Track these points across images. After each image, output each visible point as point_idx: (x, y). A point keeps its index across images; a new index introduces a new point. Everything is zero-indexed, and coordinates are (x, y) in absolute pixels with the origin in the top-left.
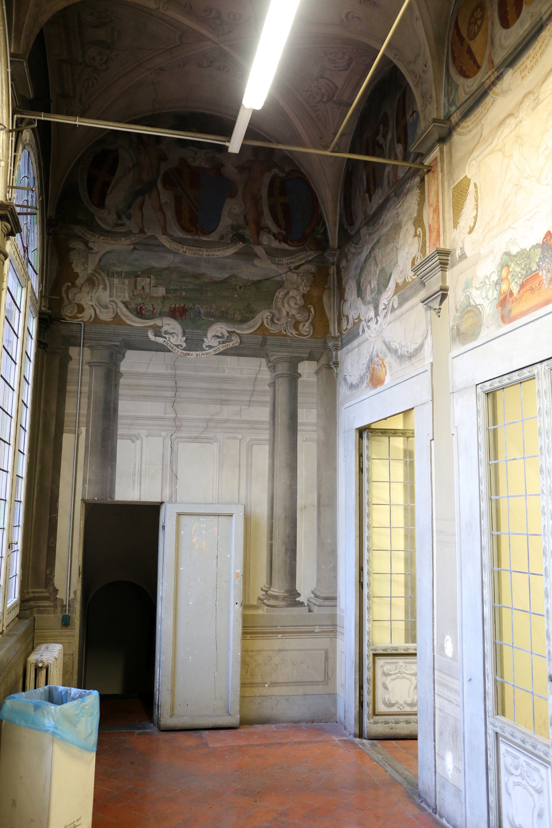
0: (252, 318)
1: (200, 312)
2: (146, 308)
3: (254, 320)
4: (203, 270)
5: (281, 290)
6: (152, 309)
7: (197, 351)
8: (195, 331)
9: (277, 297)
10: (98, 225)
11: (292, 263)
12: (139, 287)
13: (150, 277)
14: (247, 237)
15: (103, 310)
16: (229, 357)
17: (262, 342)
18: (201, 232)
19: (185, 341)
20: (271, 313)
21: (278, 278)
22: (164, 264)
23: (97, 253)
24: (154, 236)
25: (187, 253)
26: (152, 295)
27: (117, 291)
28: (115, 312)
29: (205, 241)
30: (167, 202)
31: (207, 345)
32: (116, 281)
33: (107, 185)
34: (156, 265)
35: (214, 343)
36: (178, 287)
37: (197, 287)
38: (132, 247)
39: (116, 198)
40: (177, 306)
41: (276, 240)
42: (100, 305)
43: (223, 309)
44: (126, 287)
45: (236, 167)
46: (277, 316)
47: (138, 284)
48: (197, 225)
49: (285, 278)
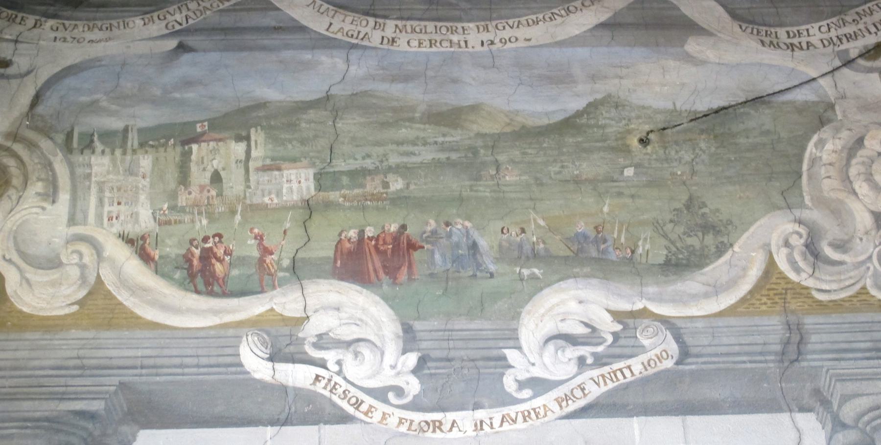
0: (721, 250)
1: (474, 247)
2: (227, 252)
4: (471, 93)
5: (826, 132)
6: (256, 254)
7: (477, 406)
8: (460, 324)
9: (814, 161)
11: (849, 38)
12: (199, 177)
13: (248, 138)
15: (36, 276)
16: (636, 426)
17: (787, 343)
19: (415, 371)
20: (800, 222)
21: (802, 95)
22: (307, 87)
23: (28, 73)
25: (402, 45)
26: (256, 200)
27: (101, 201)
28: (92, 279)
31: (523, 376)
32: (100, 164)
34: (272, 94)
35: (559, 364)
36: (369, 164)
37: (454, 156)
38: (173, 43)
40: (370, 232)
43: (581, 227)
44: (146, 182)
46: (831, 230)
47: (194, 168)
49: (831, 94)
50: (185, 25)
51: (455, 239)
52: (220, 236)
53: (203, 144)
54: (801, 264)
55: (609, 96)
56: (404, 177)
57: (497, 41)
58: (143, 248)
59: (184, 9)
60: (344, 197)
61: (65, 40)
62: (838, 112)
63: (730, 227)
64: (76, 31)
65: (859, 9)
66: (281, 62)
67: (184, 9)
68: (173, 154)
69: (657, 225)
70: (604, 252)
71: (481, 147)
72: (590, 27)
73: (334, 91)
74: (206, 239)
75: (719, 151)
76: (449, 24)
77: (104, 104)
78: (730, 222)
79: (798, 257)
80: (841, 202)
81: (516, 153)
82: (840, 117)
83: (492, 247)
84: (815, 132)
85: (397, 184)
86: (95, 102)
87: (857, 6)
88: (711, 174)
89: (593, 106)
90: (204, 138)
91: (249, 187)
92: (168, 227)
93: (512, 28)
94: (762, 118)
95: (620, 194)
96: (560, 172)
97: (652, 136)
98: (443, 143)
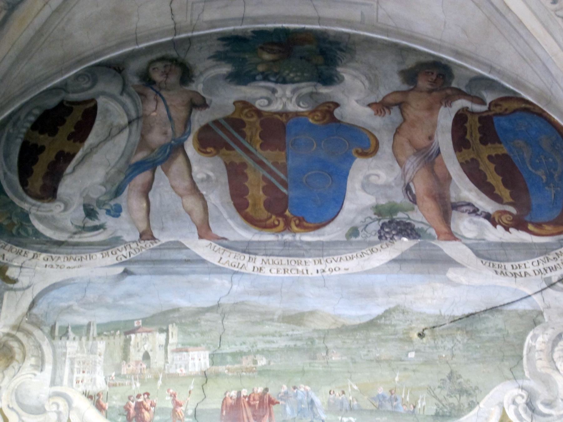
0: (472, 406)
1: (312, 403)
3: (476, 410)
4: (311, 302)
5: (538, 330)
6: (171, 406)
9: (530, 349)
10: (37, 233)
11: (551, 269)
12: (135, 355)
13: (167, 331)
14: (417, 226)
18: (297, 226)
20: (522, 388)
21: (521, 306)
23: (28, 287)
24: (178, 242)
25: (266, 270)
26: (172, 371)
27: (72, 371)
29: (309, 243)
30: (208, 177)
32: (72, 346)
33: (64, 158)
34: (183, 303)
36: (244, 348)
37: (299, 344)
38: (120, 269)
39: (84, 180)
40: (245, 392)
41: (494, 224)
42: (20, 405)
43: (381, 391)
44: (100, 359)
45: (369, 105)
46: (543, 394)
47: (132, 350)
48: (287, 213)
49: (541, 306)
50: (128, 258)
51: (299, 397)
52: (148, 394)
53: (139, 335)
54: (524, 416)
55: (398, 306)
56: (267, 357)
57: (327, 270)
58: (98, 402)
59: (128, 248)
60: (228, 369)
61: (52, 266)
62: (545, 317)
63: (477, 391)
64: (59, 261)
65: (558, 251)
66: (189, 282)
67: (128, 248)
68: (119, 340)
69: (429, 389)
70: (396, 407)
71: (317, 338)
72: (386, 261)
73: (223, 301)
74: (138, 396)
75: (470, 342)
76: (296, 259)
77: (76, 307)
78: (477, 388)
79: (521, 411)
80: (549, 375)
81: (339, 342)
82: (546, 320)
83: (323, 403)
84: (531, 330)
85: (262, 362)
86: (69, 307)
87: (556, 249)
88: (464, 356)
89: (388, 313)
90: (140, 330)
91: (167, 362)
92: (115, 388)
93: (336, 261)
94: (497, 321)
95: (405, 369)
96: (367, 355)
97: (426, 332)
98: (292, 335)
